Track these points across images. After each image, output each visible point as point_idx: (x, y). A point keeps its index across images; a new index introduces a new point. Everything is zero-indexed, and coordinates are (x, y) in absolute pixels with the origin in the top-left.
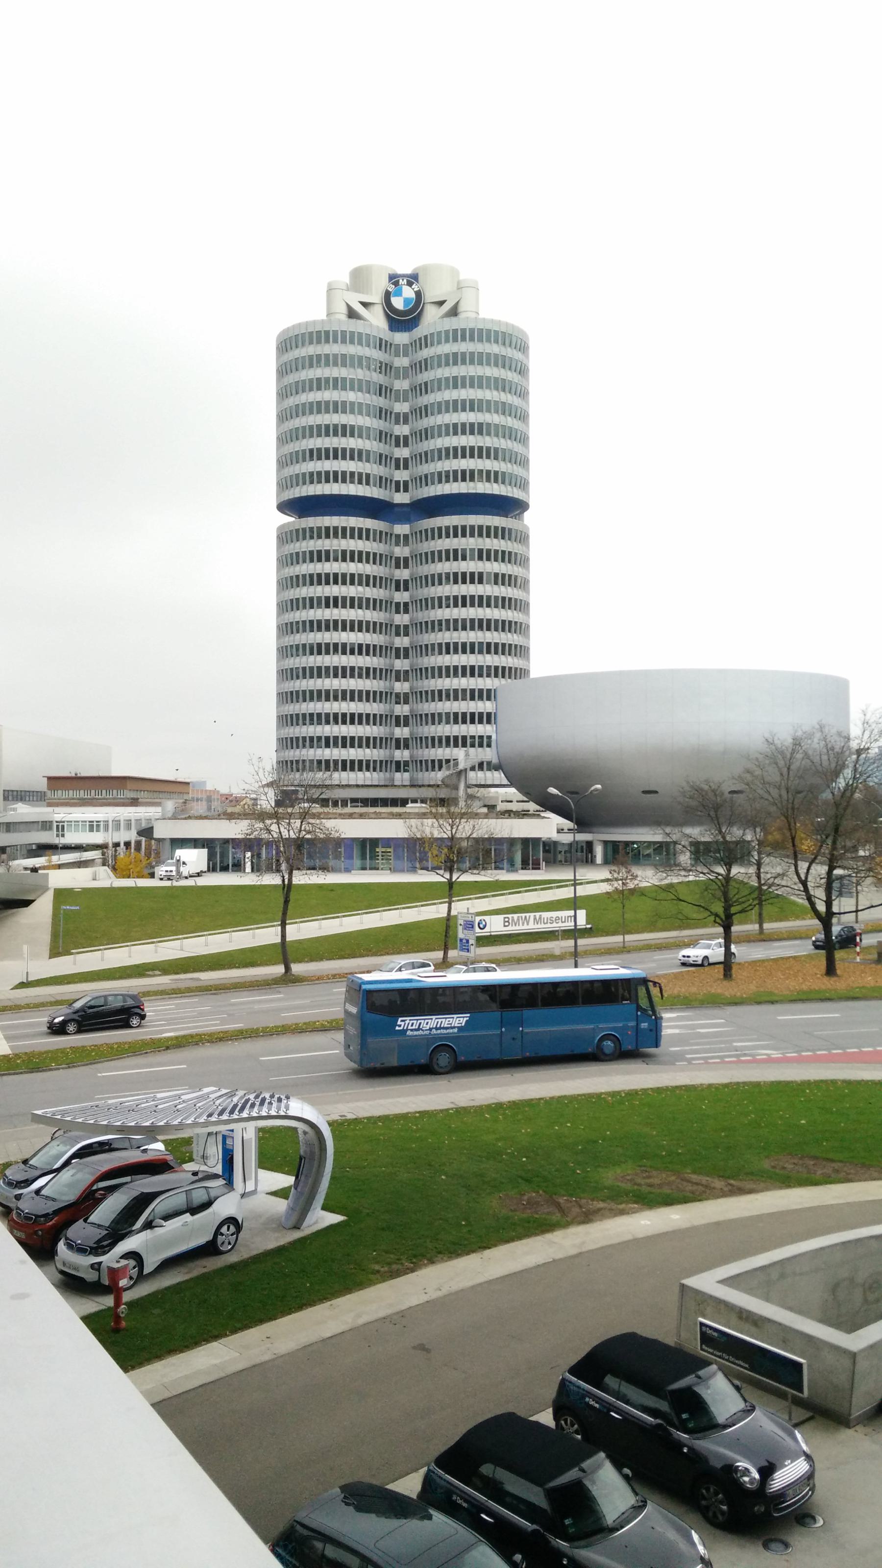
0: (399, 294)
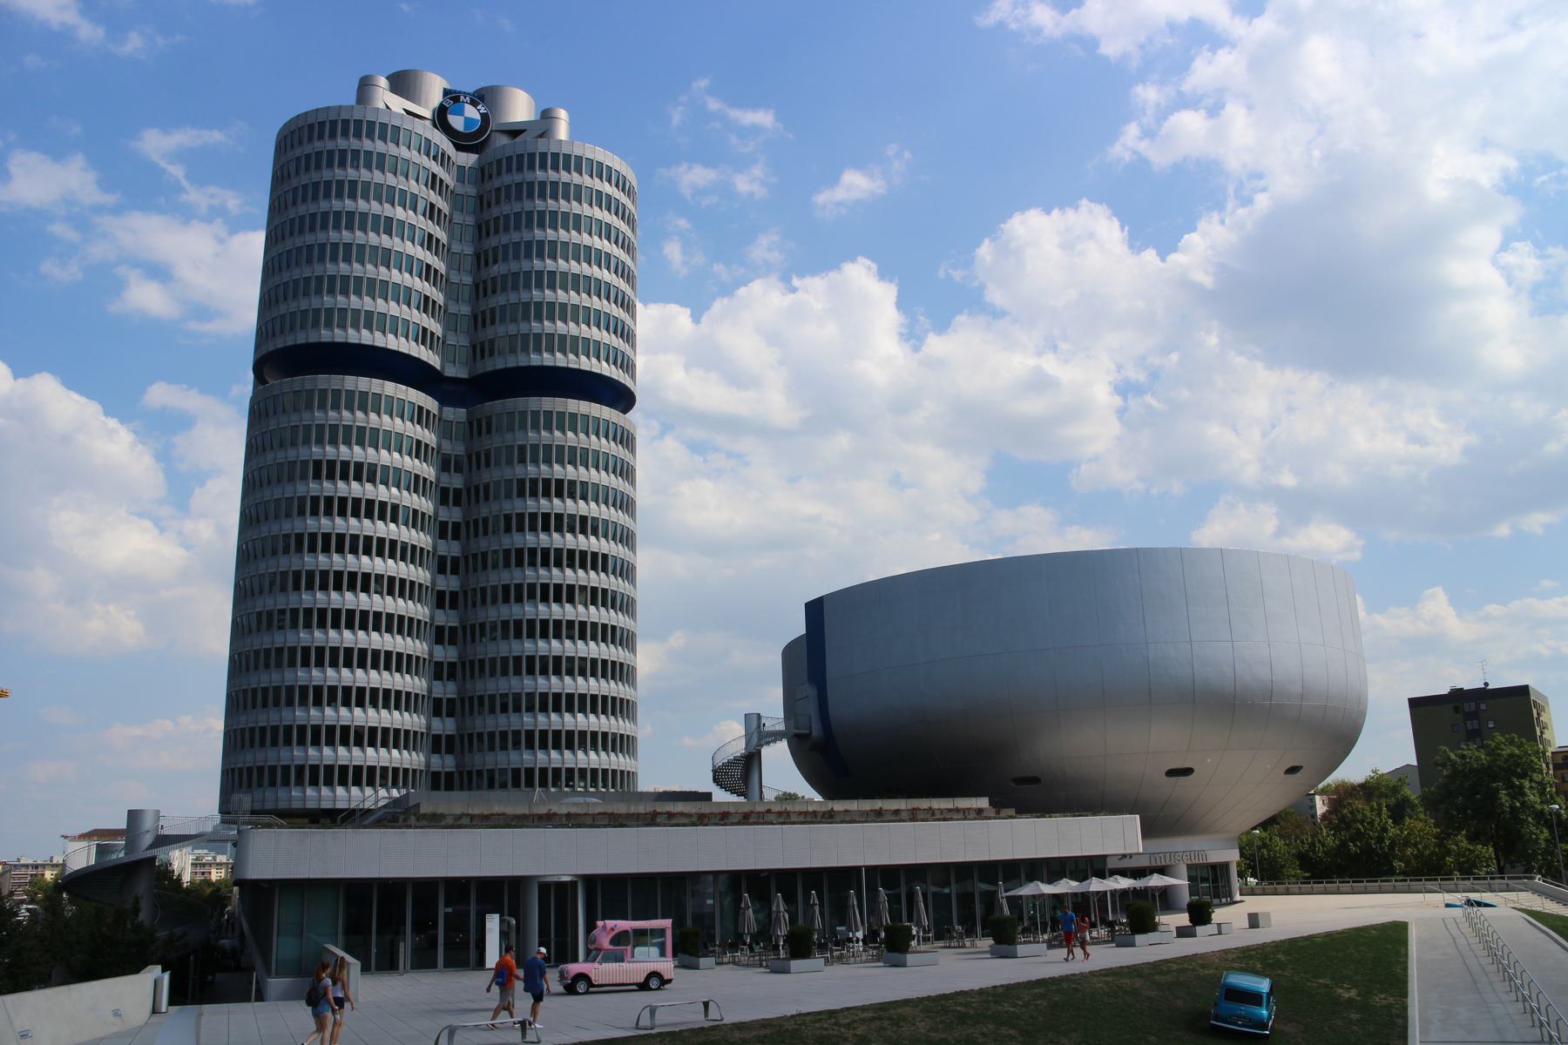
0: (461, 113)
